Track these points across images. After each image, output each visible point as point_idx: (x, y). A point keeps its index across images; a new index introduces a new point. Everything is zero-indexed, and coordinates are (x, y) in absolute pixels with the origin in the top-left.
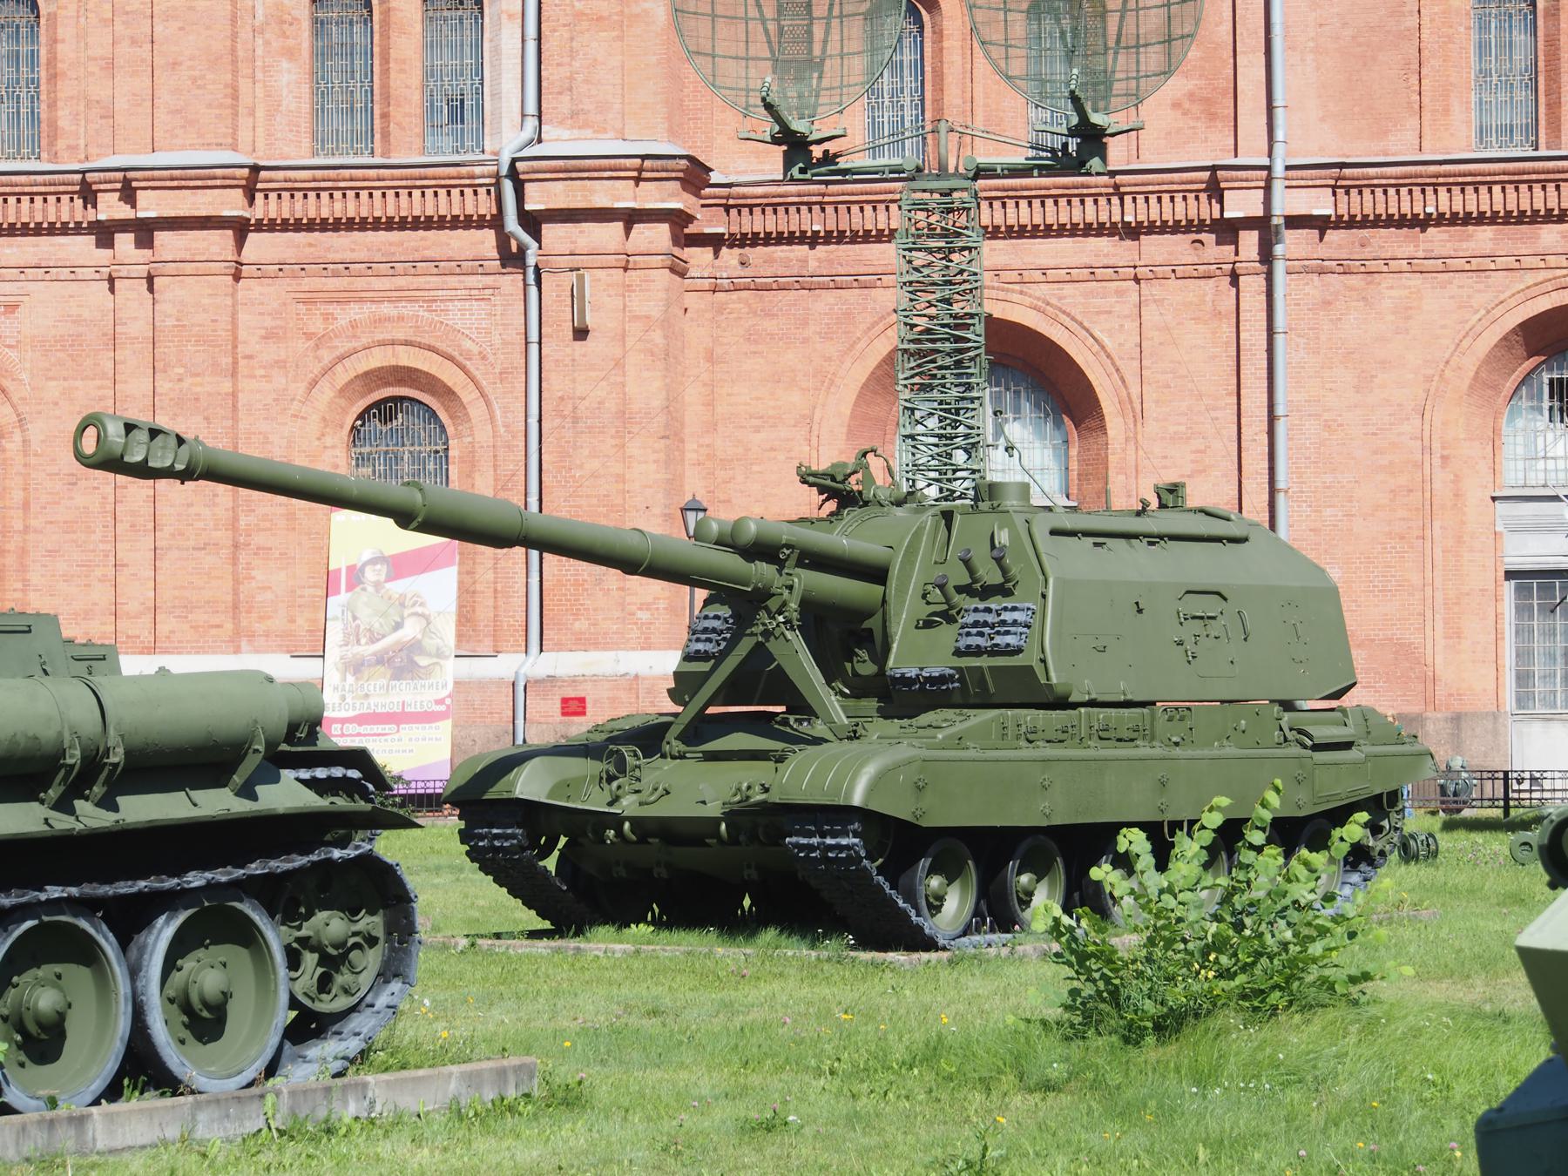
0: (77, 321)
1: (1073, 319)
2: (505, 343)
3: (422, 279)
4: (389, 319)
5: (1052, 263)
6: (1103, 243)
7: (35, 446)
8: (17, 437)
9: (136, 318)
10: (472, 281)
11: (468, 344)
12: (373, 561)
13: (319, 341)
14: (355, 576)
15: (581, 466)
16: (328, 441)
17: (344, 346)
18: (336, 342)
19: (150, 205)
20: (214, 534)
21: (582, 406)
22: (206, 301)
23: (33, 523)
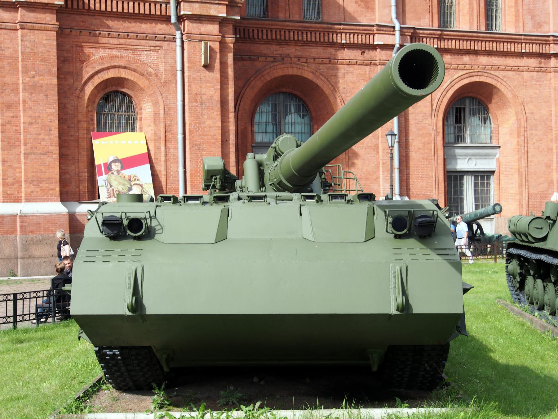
1: (325, 77)
2: (165, 70)
3: (130, 40)
4: (117, 57)
5: (317, 56)
9: (9, 48)
10: (151, 43)
11: (150, 69)
12: (114, 161)
14: (108, 168)
15: (204, 123)
16: (90, 108)
18: (95, 65)
20: (51, 148)
21: (204, 97)
22: (45, 42)
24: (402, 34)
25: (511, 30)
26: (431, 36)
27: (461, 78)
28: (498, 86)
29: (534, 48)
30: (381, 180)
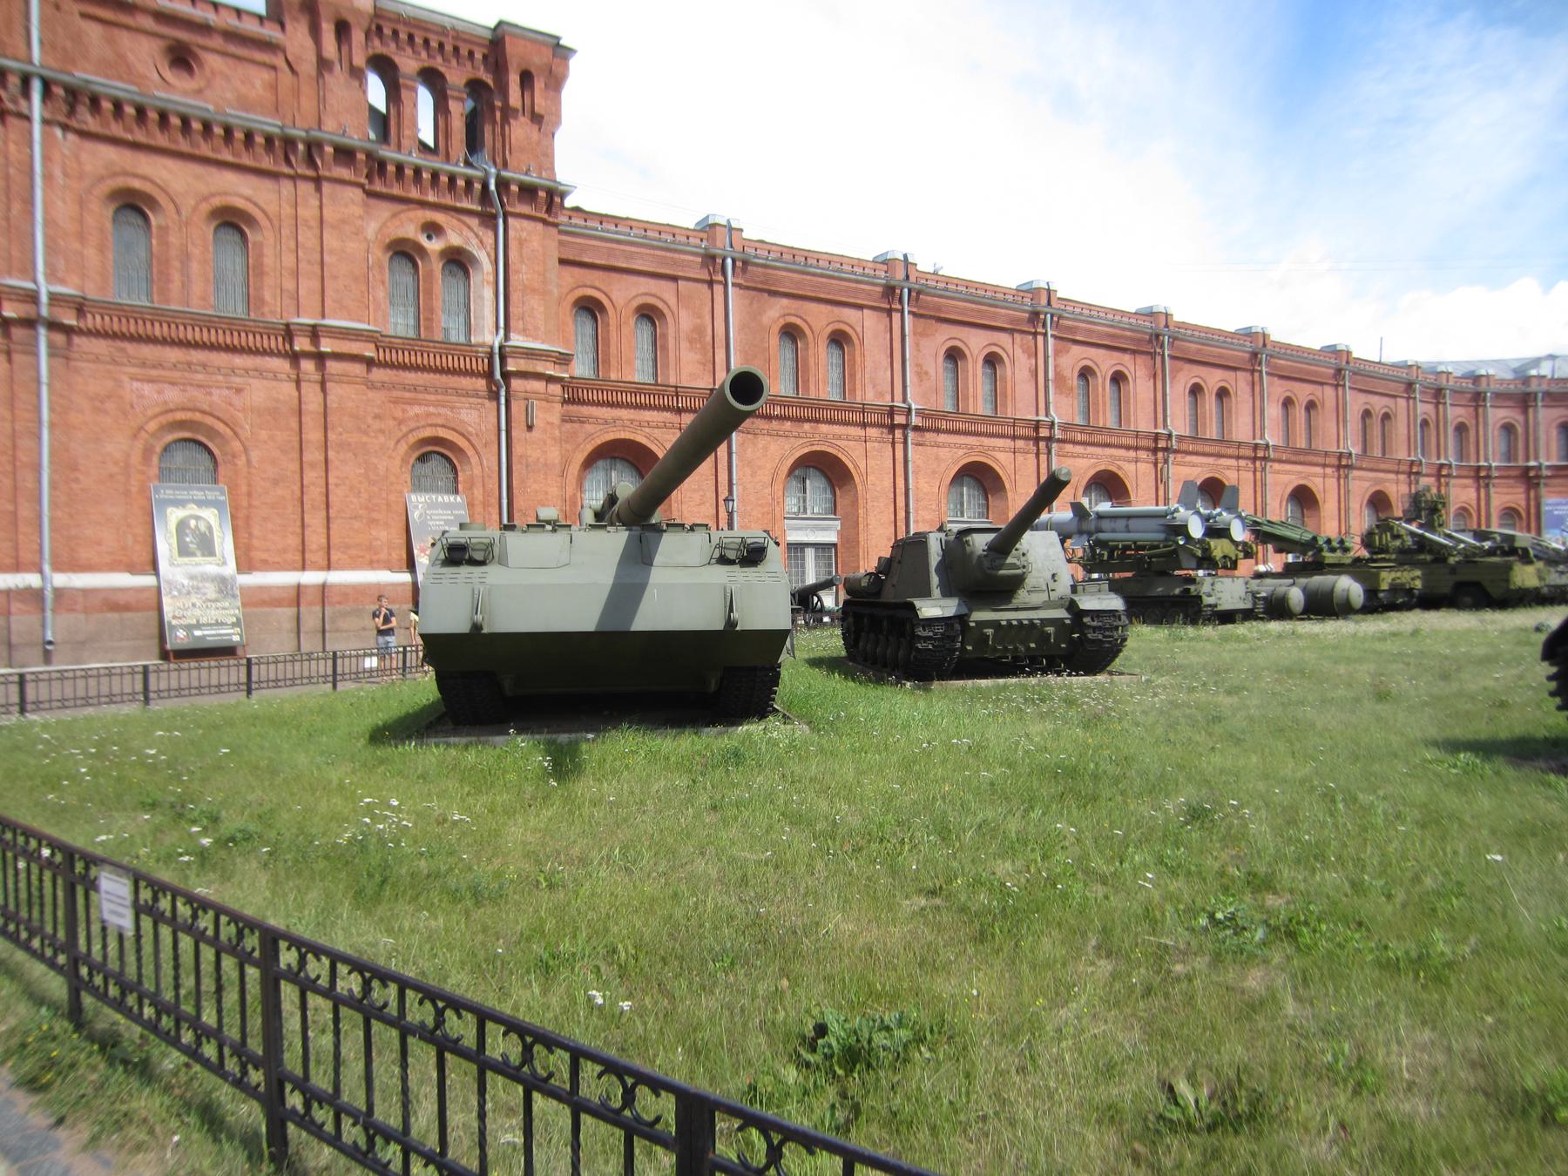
0: (277, 400)
6: (667, 415)
7: (255, 463)
8: (244, 458)
10: (471, 400)
13: (400, 422)
17: (413, 425)
19: (326, 346)
23: (256, 503)
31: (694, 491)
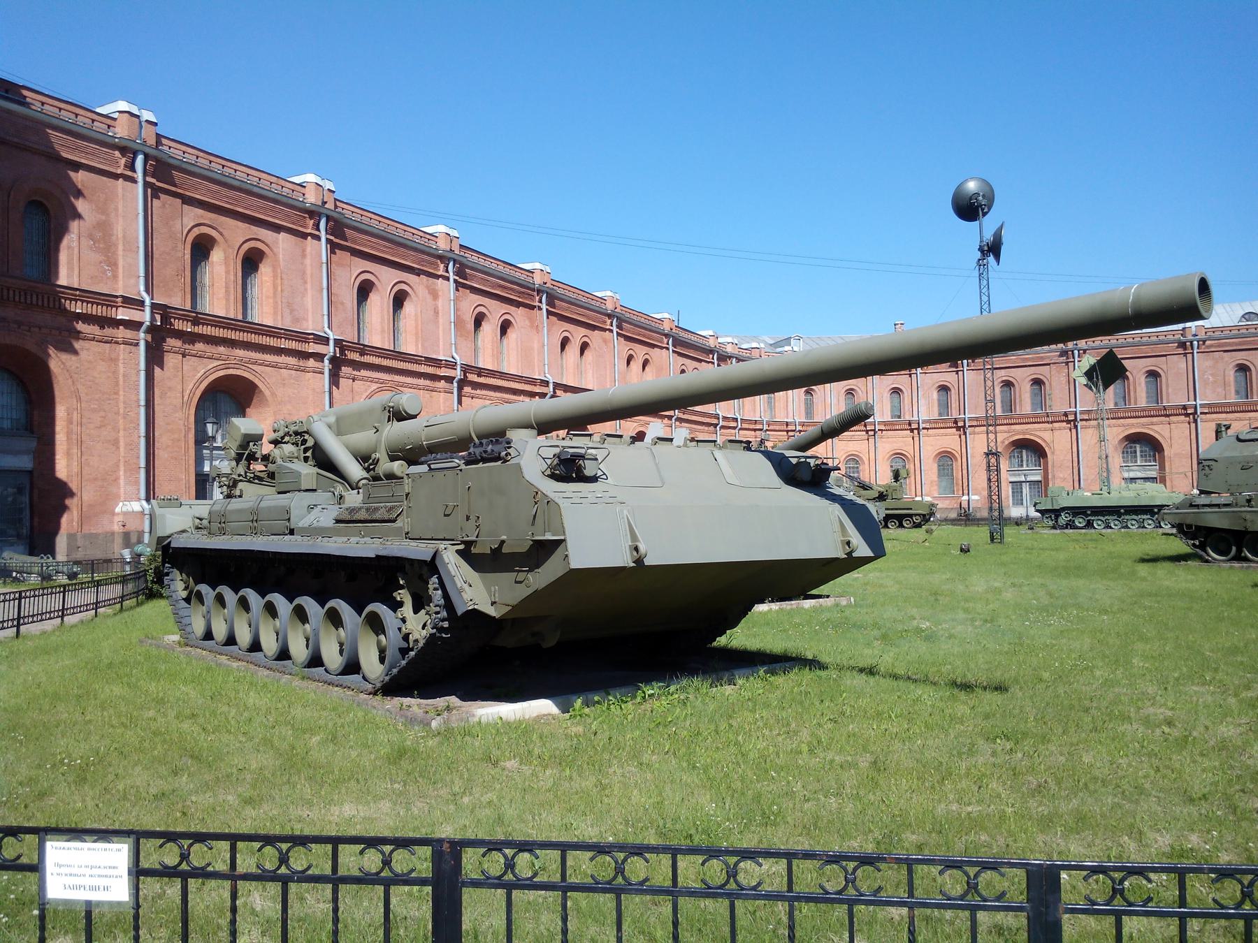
24: (152, 313)
25: (268, 321)
26: (184, 318)
27: (216, 369)
28: (256, 381)
29: (293, 345)
30: (122, 482)
31: (94, 411)
